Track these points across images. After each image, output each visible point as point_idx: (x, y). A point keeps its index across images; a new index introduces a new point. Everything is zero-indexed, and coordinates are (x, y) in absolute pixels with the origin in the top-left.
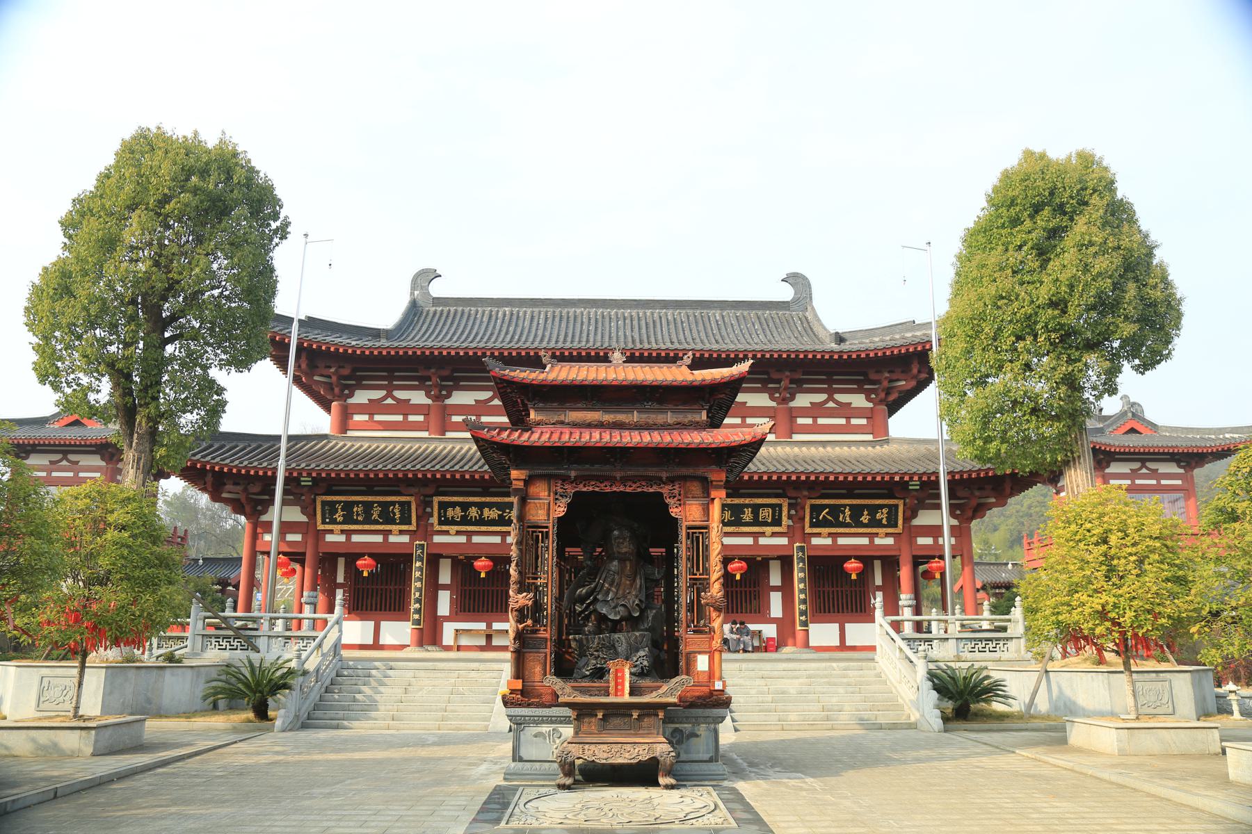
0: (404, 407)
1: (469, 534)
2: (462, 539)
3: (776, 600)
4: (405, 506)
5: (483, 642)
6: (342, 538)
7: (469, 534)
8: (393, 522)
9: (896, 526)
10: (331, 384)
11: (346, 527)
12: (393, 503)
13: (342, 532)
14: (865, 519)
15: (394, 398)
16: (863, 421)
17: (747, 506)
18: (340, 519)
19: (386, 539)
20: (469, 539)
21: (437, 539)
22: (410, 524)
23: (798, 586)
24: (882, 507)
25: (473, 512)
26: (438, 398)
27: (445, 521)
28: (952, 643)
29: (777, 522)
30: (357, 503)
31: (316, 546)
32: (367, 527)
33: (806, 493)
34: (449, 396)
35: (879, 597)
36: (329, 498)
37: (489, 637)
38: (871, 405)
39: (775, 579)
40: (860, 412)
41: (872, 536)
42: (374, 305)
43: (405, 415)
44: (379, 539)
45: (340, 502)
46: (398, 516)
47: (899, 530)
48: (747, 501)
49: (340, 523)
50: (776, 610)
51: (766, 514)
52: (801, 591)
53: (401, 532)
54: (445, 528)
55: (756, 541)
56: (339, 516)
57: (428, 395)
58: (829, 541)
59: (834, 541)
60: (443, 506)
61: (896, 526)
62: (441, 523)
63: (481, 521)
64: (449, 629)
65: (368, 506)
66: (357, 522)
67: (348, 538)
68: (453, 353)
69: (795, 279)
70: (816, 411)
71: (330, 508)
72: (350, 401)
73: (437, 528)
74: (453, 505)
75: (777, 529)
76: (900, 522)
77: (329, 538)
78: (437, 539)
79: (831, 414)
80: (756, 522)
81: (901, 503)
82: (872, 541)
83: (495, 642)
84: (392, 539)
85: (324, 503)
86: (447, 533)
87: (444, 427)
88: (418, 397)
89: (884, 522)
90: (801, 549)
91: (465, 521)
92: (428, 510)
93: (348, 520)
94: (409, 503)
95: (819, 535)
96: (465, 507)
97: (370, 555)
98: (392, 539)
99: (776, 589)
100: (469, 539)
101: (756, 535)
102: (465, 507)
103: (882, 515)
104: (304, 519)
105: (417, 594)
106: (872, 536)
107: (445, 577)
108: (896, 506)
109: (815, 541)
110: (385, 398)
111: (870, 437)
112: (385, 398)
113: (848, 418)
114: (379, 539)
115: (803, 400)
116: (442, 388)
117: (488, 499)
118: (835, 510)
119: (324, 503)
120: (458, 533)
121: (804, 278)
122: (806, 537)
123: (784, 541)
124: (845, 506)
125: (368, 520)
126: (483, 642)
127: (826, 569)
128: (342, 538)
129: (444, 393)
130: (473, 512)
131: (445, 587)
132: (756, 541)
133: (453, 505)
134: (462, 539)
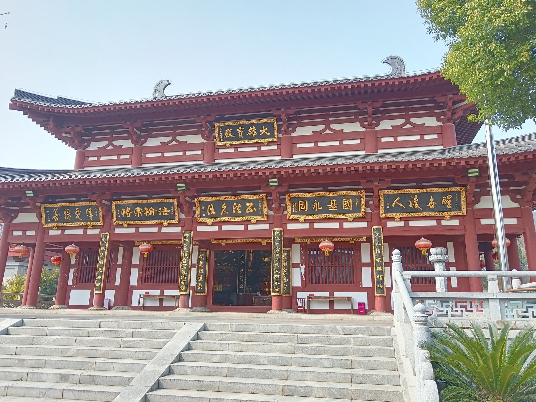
1: (137, 227)
2: (133, 230)
5: (156, 304)
6: (58, 232)
7: (137, 227)
11: (60, 225)
12: (88, 207)
13: (58, 228)
14: (431, 204)
15: (113, 145)
16: (435, 136)
17: (332, 198)
20: (137, 230)
21: (117, 231)
24: (445, 194)
25: (138, 211)
28: (494, 306)
29: (357, 210)
31: (43, 238)
32: (73, 224)
33: (376, 183)
37: (161, 301)
38: (441, 124)
40: (431, 130)
44: (81, 232)
45: (56, 208)
48: (332, 194)
49: (56, 222)
51: (347, 203)
53: (94, 227)
54: (121, 223)
55: (341, 225)
56: (56, 218)
58: (402, 224)
59: (406, 224)
60: (119, 207)
61: (460, 210)
63: (144, 217)
64: (136, 295)
66: (67, 221)
67: (63, 233)
70: (395, 132)
71: (50, 212)
74: (125, 206)
75: (357, 215)
76: (464, 207)
77: (52, 232)
78: (117, 231)
80: (339, 210)
81: (463, 190)
88: (127, 144)
89: (449, 206)
91: (133, 217)
95: (392, 219)
96: (133, 207)
97: (76, 244)
100: (137, 230)
103: (447, 201)
104: (38, 221)
105: (100, 269)
106: (439, 219)
108: (459, 193)
109: (390, 224)
111: (441, 147)
112: (108, 146)
113: (422, 135)
114: (81, 232)
115: (386, 125)
118: (405, 199)
119: (46, 209)
120: (129, 226)
121: (398, 58)
122: (382, 222)
123: (364, 225)
125: (73, 220)
128: (58, 232)
130: (138, 211)
131: (135, 266)
132: (341, 225)
133: (125, 206)
134: (133, 230)
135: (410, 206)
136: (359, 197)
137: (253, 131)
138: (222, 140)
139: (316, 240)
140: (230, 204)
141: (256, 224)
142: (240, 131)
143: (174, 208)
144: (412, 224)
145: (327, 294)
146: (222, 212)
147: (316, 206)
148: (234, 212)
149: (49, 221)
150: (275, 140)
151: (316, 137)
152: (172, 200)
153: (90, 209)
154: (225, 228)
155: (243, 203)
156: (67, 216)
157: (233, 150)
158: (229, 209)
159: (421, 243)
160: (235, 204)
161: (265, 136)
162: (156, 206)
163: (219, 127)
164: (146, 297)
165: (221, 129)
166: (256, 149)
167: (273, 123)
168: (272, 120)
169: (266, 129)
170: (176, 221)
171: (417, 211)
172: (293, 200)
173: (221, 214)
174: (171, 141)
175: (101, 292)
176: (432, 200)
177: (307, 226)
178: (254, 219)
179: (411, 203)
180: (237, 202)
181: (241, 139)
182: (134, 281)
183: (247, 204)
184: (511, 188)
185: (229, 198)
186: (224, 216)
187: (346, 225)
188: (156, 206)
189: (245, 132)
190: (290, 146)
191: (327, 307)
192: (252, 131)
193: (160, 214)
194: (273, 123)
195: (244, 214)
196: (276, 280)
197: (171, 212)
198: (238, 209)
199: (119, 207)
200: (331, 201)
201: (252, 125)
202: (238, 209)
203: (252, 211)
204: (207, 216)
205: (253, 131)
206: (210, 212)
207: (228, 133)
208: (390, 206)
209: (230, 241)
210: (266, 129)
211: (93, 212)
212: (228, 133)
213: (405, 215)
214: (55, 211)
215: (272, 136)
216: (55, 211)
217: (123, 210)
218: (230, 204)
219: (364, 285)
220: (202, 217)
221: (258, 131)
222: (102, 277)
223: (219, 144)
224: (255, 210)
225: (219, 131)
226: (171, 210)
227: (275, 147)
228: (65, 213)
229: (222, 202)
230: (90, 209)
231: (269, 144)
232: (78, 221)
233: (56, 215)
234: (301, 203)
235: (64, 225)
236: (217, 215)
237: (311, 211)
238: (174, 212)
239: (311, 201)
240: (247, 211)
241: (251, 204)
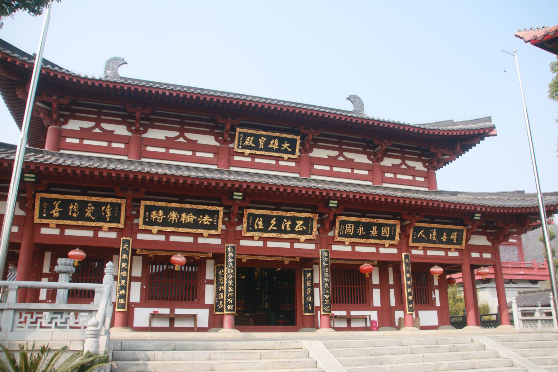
0: (110, 137)
2: (162, 238)
3: (376, 294)
4: (116, 208)
5: (166, 324)
6: (57, 232)
8: (104, 220)
9: (461, 244)
10: (51, 111)
11: (61, 222)
12: (106, 204)
13: (58, 226)
14: (444, 238)
15: (101, 128)
16: (422, 179)
18: (56, 215)
19: (96, 234)
21: (140, 237)
22: (119, 222)
23: (406, 283)
24: (454, 230)
25: (173, 216)
26: (137, 131)
27: (149, 222)
29: (392, 237)
30: (74, 202)
32: (80, 223)
34: (145, 131)
35: (437, 291)
36: (48, 196)
39: (376, 280)
41: (447, 250)
42: (85, 63)
43: (110, 142)
44: (89, 234)
45: (57, 200)
46: (109, 215)
47: (463, 247)
48: (375, 221)
50: (377, 301)
51: (386, 231)
52: (408, 287)
53: (111, 229)
54: (148, 228)
55: (378, 250)
56: (55, 213)
57: (129, 130)
58: (421, 253)
60: (149, 209)
61: (461, 244)
62: (145, 223)
63: (179, 224)
65: (83, 205)
66: (72, 218)
67: (62, 232)
68: (160, 92)
69: (352, 99)
70: (395, 169)
72: (64, 127)
73: (142, 227)
74: (157, 209)
75: (392, 242)
76: (464, 242)
78: (140, 237)
79: (404, 172)
80: (379, 237)
82: (446, 254)
83: (177, 324)
84: (101, 234)
85: (43, 200)
86: (150, 232)
87: (142, 154)
88: (121, 130)
89: (455, 241)
90: (406, 257)
91: (166, 222)
92: (134, 212)
93: (64, 215)
94: (119, 205)
95: (417, 248)
96: (167, 211)
97: (82, 248)
98: (101, 234)
99: (376, 286)
101: (378, 246)
102: (167, 211)
103: (453, 237)
105: (123, 282)
106: (447, 250)
107: (137, 272)
109: (414, 252)
110: (94, 128)
112: (94, 128)
114: (89, 234)
115: (387, 162)
116: (142, 125)
117: (186, 206)
118: (428, 231)
119: (43, 200)
120: (160, 232)
121: (359, 99)
123: (394, 251)
124: (433, 228)
125: (82, 217)
126: (166, 324)
127: (421, 270)
128: (57, 232)
129: (142, 129)
130: (173, 216)
133: (157, 209)
134: (162, 238)
135: (430, 237)
136: (395, 226)
137: (274, 144)
138: (240, 147)
139: (168, 254)
140: (280, 220)
141: (304, 243)
142: (262, 141)
143: (218, 217)
144: (430, 253)
145: (344, 313)
146: (271, 227)
147: (361, 230)
148: (283, 228)
149: (45, 215)
150: (295, 157)
151: (331, 162)
152: (217, 208)
153: (109, 206)
154: (270, 244)
155: (294, 220)
156: (73, 212)
157: (249, 159)
158: (278, 225)
159: (366, 266)
160: (285, 220)
161: (286, 151)
162: (198, 213)
163: (240, 133)
164: (154, 316)
165: (241, 135)
166: (273, 162)
167: (296, 140)
168: (296, 137)
169: (289, 145)
170: (218, 232)
171: (434, 242)
172: (343, 223)
173: (270, 229)
174: (178, 137)
175: (126, 310)
176: (445, 234)
177: (260, 244)
178: (303, 237)
179: (431, 235)
180: (288, 218)
181: (261, 150)
182: (135, 295)
183: (298, 222)
184: (488, 231)
185: (280, 214)
186: (272, 231)
187: (382, 250)
188: (198, 213)
189: (267, 143)
190: (306, 164)
191: (345, 325)
192: (274, 143)
193: (200, 222)
194: (296, 140)
195: (293, 231)
196: (327, 299)
197: (213, 222)
198: (288, 226)
199: (149, 209)
200: (373, 227)
201: (275, 138)
202: (288, 226)
203: (301, 229)
204: (254, 230)
205: (274, 144)
206: (258, 225)
207: (249, 141)
208: (417, 237)
209: (251, 258)
210: (289, 145)
211: (112, 212)
212: (249, 141)
213: (426, 245)
214: (57, 204)
215: (293, 152)
216: (57, 204)
217: (154, 212)
218: (280, 220)
219: (374, 305)
220: (248, 230)
221: (280, 145)
222: (126, 291)
223: (236, 150)
224: (305, 228)
225: (240, 137)
226: (214, 219)
227: (293, 164)
228: (71, 207)
229: (272, 217)
230: (109, 206)
231: (289, 160)
232: (89, 219)
233: (57, 209)
234: (348, 226)
235: (168, 230)
236: (265, 230)
237: (356, 235)
238: (217, 222)
239: (357, 224)
240: (296, 229)
241: (301, 222)
